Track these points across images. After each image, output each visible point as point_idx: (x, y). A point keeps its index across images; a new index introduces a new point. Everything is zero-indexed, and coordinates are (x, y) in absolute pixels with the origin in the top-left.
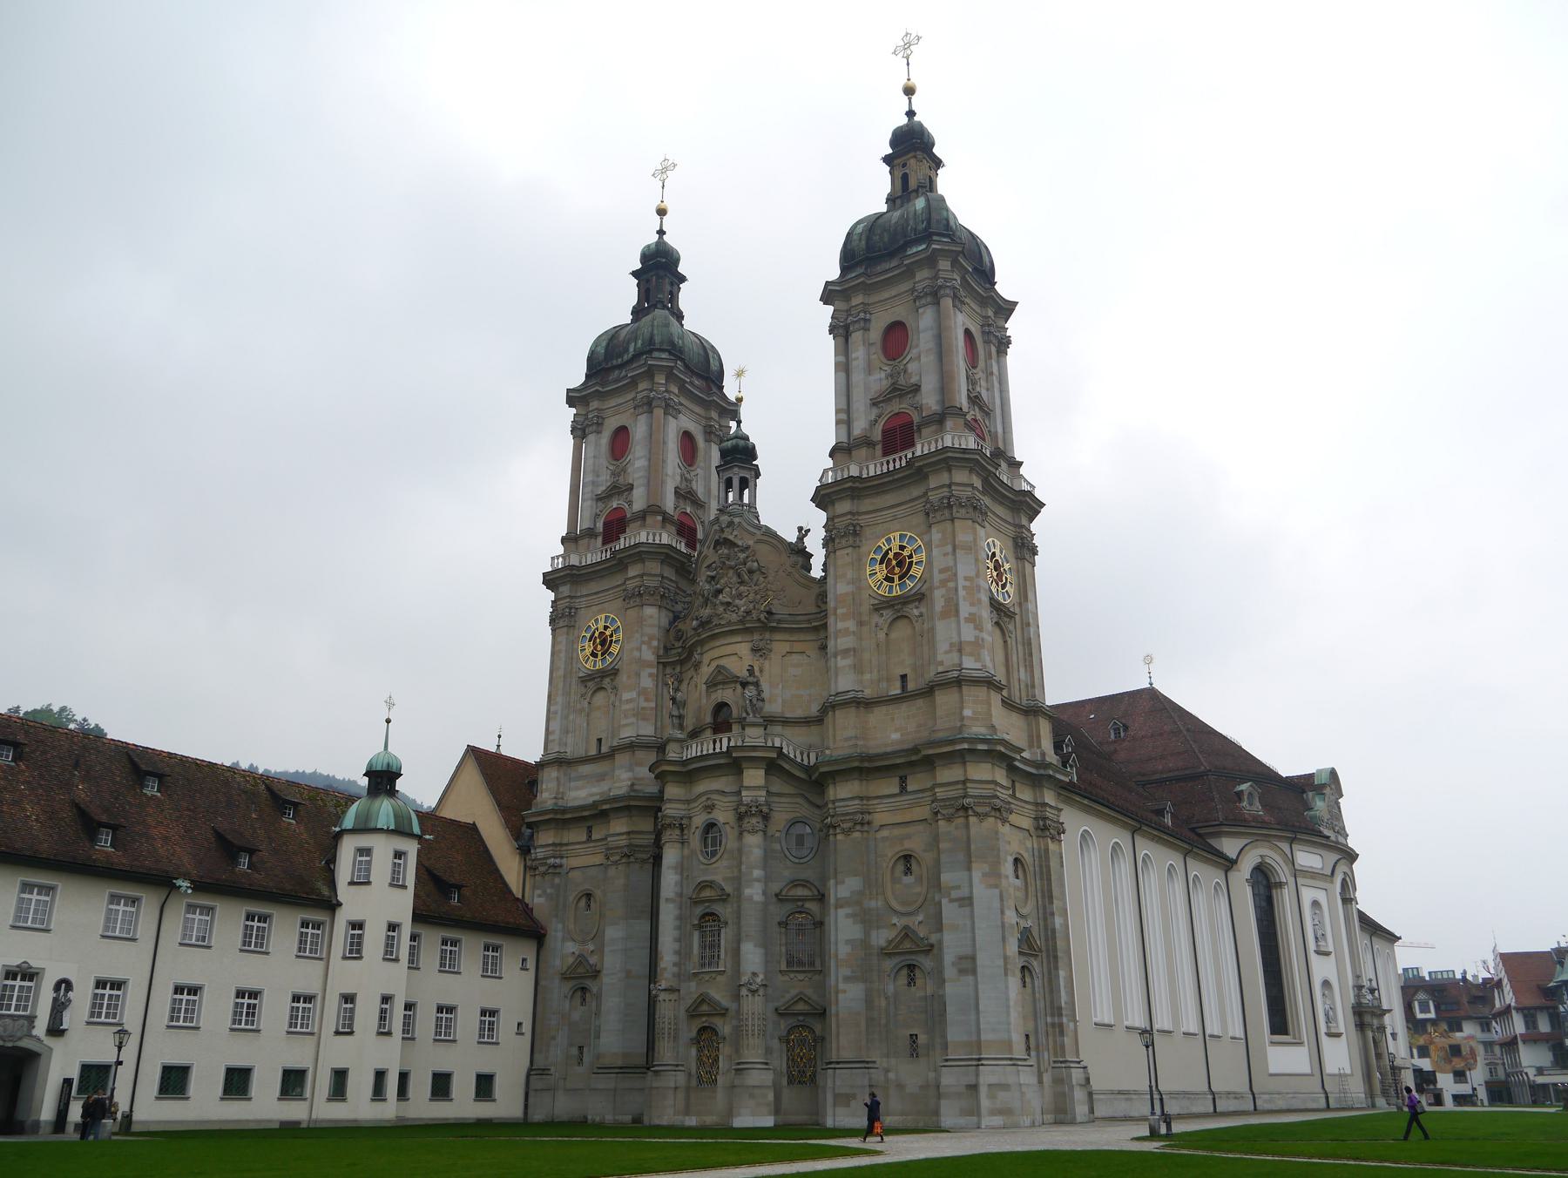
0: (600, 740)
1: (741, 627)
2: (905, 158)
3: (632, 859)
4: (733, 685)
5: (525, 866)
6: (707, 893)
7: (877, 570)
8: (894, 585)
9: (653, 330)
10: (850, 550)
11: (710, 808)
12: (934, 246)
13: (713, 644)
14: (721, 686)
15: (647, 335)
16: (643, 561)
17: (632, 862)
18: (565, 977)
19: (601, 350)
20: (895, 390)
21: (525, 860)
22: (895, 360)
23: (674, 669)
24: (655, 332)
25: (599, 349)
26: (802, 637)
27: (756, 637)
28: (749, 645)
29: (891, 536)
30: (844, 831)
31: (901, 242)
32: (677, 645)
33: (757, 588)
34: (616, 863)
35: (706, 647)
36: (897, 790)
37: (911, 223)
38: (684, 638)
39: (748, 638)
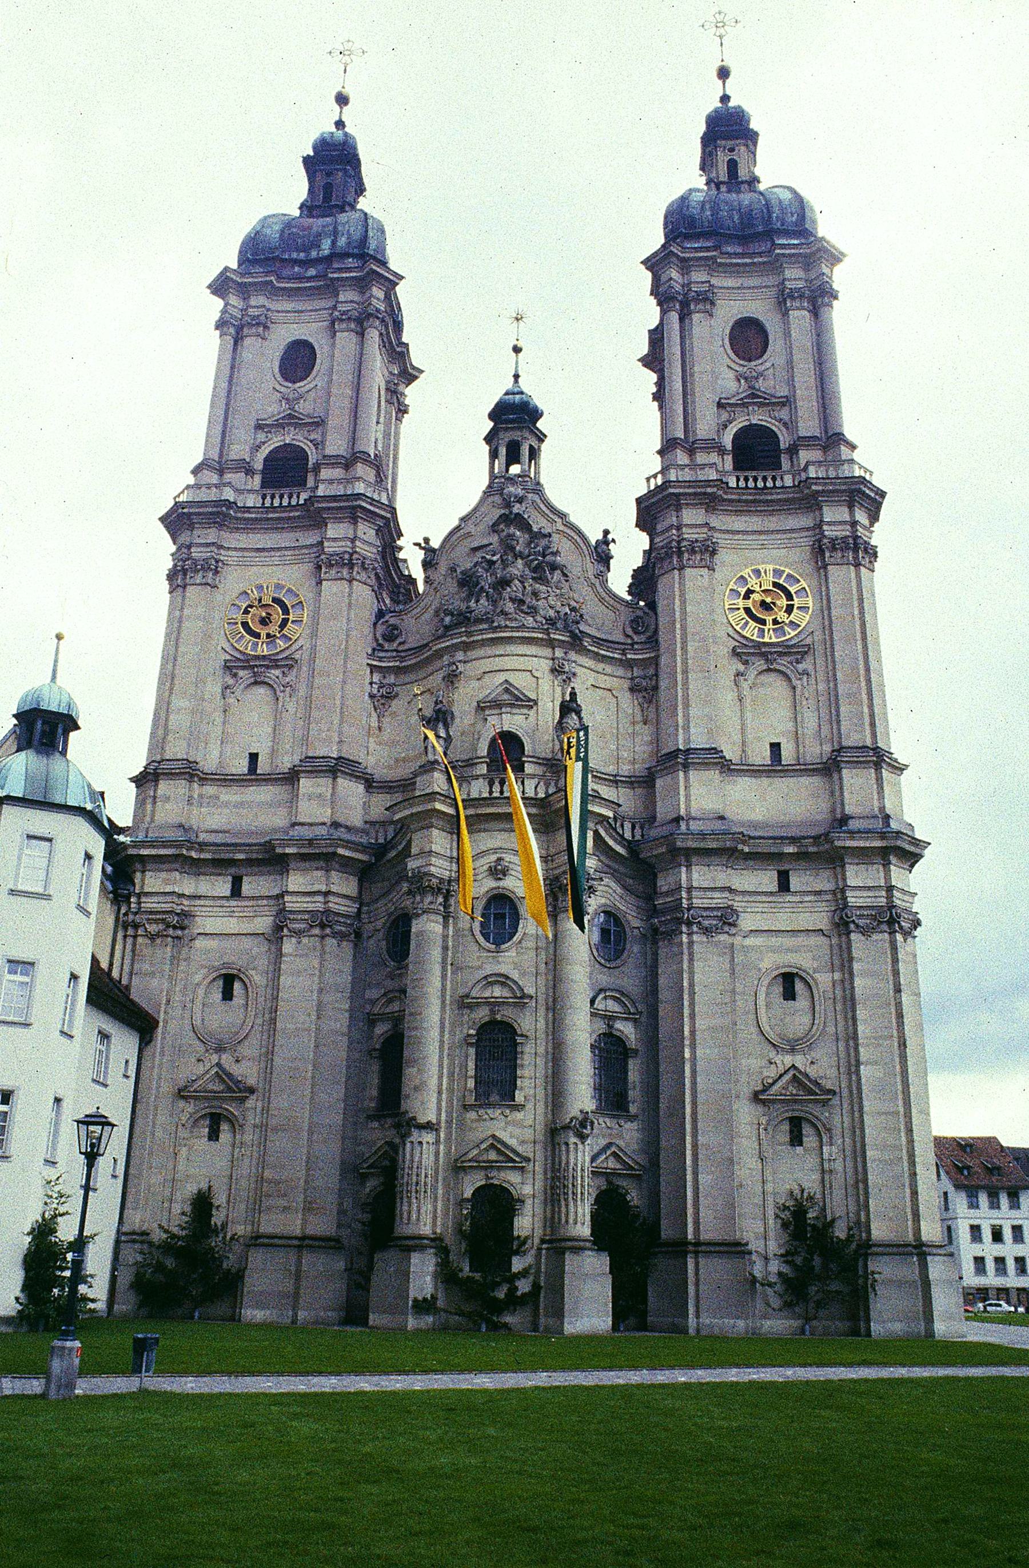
0: (254, 757)
1: (545, 637)
2: (738, 142)
3: (328, 931)
4: (525, 711)
5: (117, 919)
6: (497, 991)
7: (741, 606)
8: (766, 628)
9: (366, 231)
10: (705, 571)
11: (498, 871)
12: (778, 251)
13: (489, 651)
14: (508, 709)
15: (357, 235)
16: (354, 520)
17: (328, 935)
18: (182, 1094)
19: (273, 233)
20: (754, 396)
21: (119, 910)
22: (750, 360)
23: (384, 677)
24: (371, 234)
25: (268, 231)
26: (609, 669)
27: (559, 653)
28: (545, 665)
29: (760, 567)
30: (707, 931)
31: (760, 228)
32: (386, 646)
33: (558, 591)
34: (298, 933)
35: (472, 654)
36: (774, 887)
37: (776, 209)
38: (400, 640)
39: (547, 652)
